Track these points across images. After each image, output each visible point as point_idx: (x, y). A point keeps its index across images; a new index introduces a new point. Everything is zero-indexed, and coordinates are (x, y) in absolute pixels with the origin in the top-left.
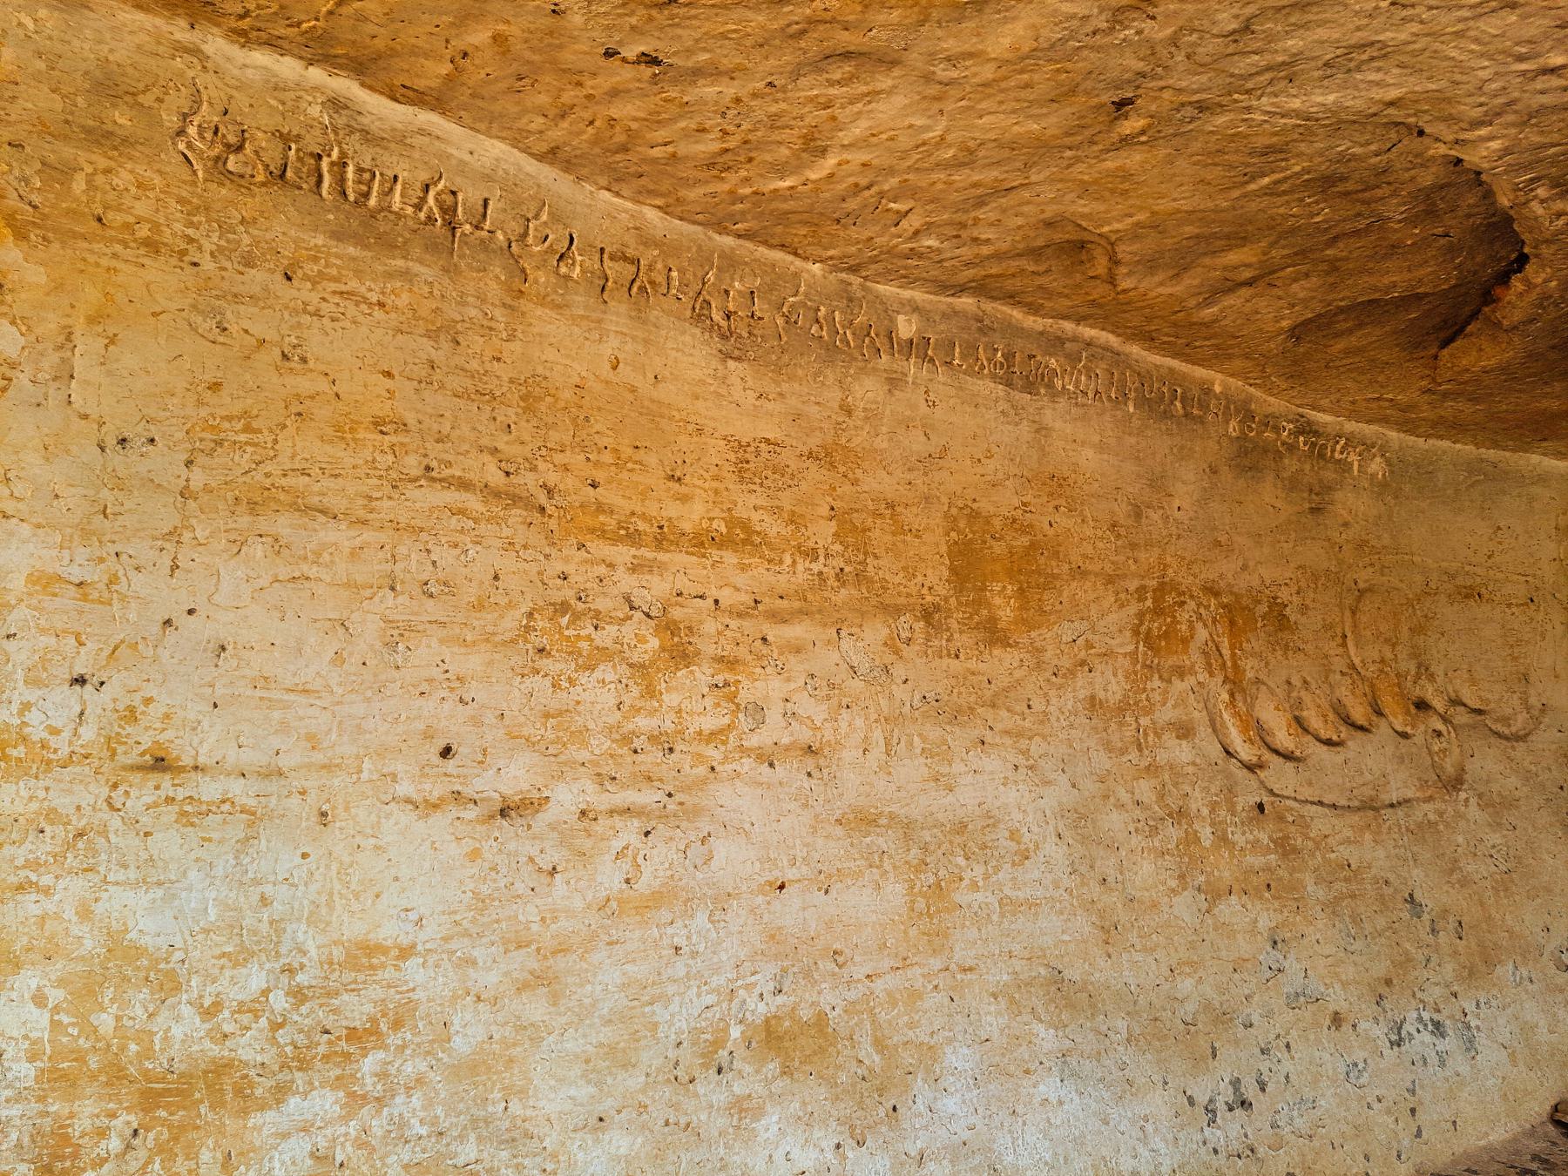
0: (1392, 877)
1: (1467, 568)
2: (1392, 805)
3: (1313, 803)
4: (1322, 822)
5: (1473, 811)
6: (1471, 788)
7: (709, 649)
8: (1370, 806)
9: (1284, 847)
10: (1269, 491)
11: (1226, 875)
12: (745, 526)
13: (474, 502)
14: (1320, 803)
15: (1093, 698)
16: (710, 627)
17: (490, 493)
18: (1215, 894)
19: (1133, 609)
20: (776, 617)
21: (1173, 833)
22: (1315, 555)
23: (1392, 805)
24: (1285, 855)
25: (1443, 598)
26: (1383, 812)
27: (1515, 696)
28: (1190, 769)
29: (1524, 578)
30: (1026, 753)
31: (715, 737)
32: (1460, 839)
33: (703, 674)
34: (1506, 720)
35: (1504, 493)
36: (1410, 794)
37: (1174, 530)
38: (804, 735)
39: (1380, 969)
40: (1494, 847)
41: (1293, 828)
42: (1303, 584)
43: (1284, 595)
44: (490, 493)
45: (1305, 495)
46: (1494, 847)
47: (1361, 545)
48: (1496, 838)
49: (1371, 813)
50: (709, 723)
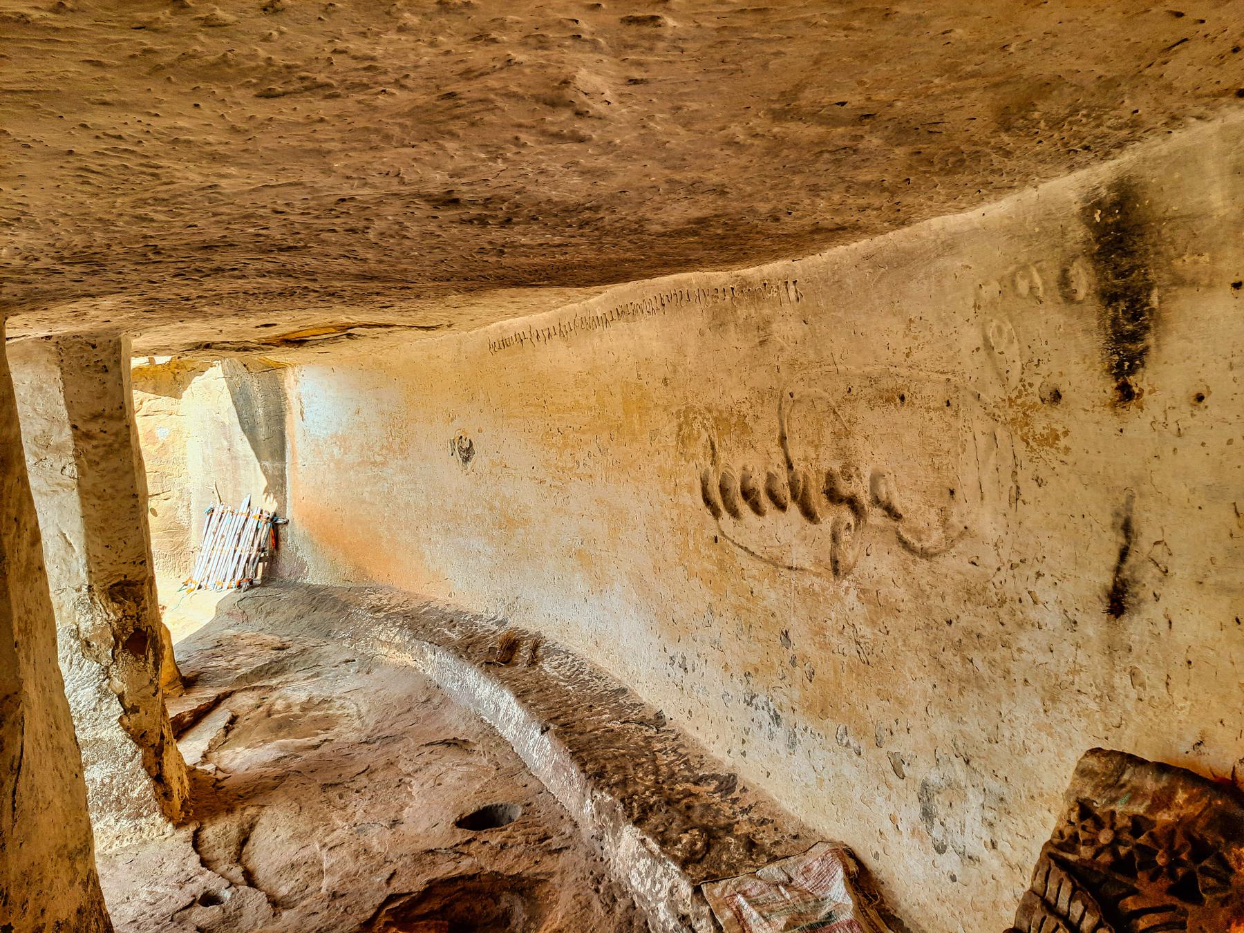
0: (778, 614)
1: (892, 370)
2: (790, 568)
3: (741, 547)
4: (743, 560)
5: (852, 597)
6: (856, 581)
7: (570, 443)
8: (774, 562)
9: (721, 565)
10: (733, 337)
11: (696, 568)
12: (577, 402)
13: (533, 409)
14: (746, 549)
15: (661, 466)
16: (571, 436)
17: (536, 405)
18: (691, 574)
19: (675, 423)
20: (584, 433)
21: (680, 538)
22: (762, 378)
23: (790, 568)
24: (721, 569)
25: (862, 405)
26: (780, 569)
27: (933, 510)
28: (690, 509)
29: (943, 377)
30: (637, 487)
31: (571, 469)
32: (833, 615)
33: (569, 450)
34: (918, 533)
35: (910, 277)
36: (807, 565)
37: (689, 377)
38: (589, 472)
39: (754, 659)
40: (863, 637)
41: (727, 557)
42: (753, 401)
43: (745, 409)
44: (536, 405)
45: (756, 333)
46: (863, 637)
47: (792, 364)
48: (866, 631)
49: (771, 567)
50: (570, 465)
